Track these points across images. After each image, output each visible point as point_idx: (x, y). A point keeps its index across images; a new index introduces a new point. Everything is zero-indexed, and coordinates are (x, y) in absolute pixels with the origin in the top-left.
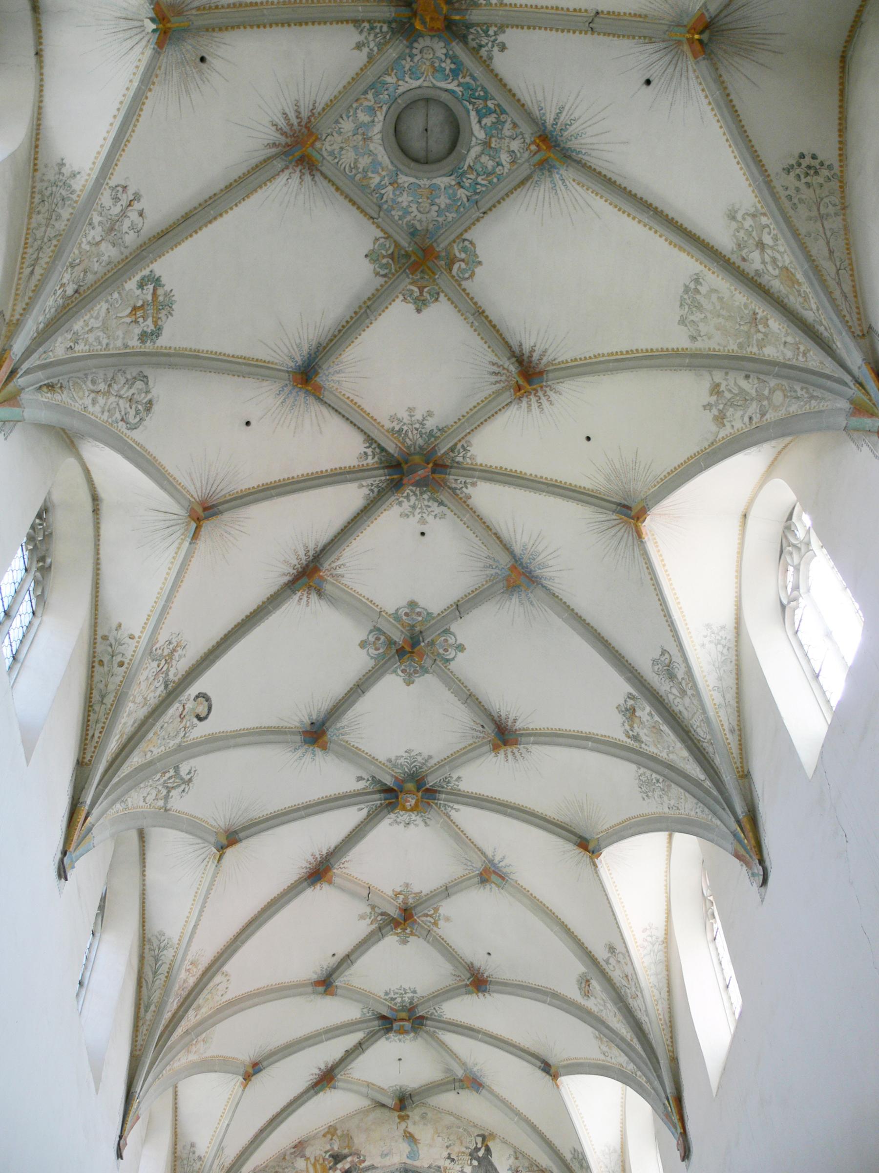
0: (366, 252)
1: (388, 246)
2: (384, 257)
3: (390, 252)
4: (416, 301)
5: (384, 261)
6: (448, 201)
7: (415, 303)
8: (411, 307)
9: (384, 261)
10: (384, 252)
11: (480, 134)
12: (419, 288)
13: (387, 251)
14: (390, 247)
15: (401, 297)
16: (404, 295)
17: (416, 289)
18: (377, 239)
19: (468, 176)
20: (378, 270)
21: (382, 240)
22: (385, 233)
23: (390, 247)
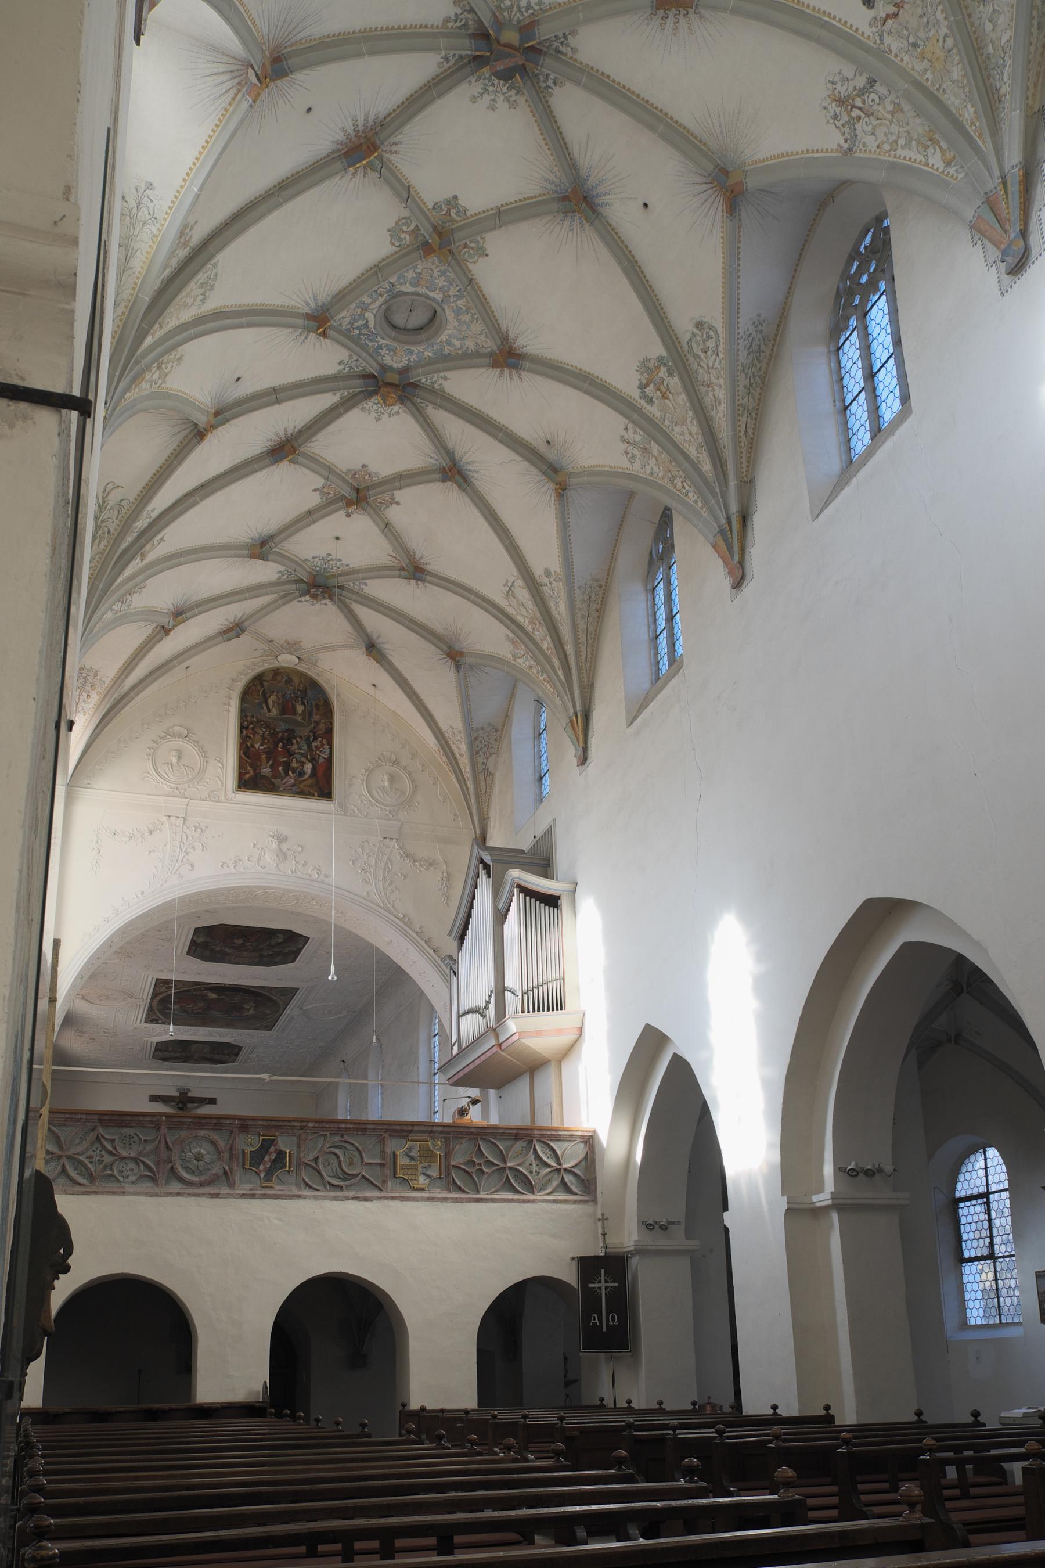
0: (486, 257)
1: (466, 255)
2: (473, 248)
3: (466, 250)
4: (456, 206)
5: (473, 245)
6: (406, 274)
7: (457, 204)
8: (461, 202)
9: (473, 245)
10: (471, 251)
11: (369, 315)
12: (450, 215)
13: (469, 251)
14: (465, 253)
15: (468, 214)
16: (465, 214)
17: (453, 215)
18: (474, 263)
19: (385, 290)
20: (481, 241)
21: (470, 261)
22: (466, 264)
23: (465, 253)
